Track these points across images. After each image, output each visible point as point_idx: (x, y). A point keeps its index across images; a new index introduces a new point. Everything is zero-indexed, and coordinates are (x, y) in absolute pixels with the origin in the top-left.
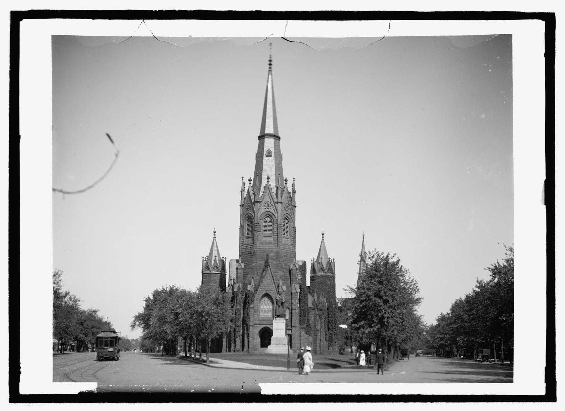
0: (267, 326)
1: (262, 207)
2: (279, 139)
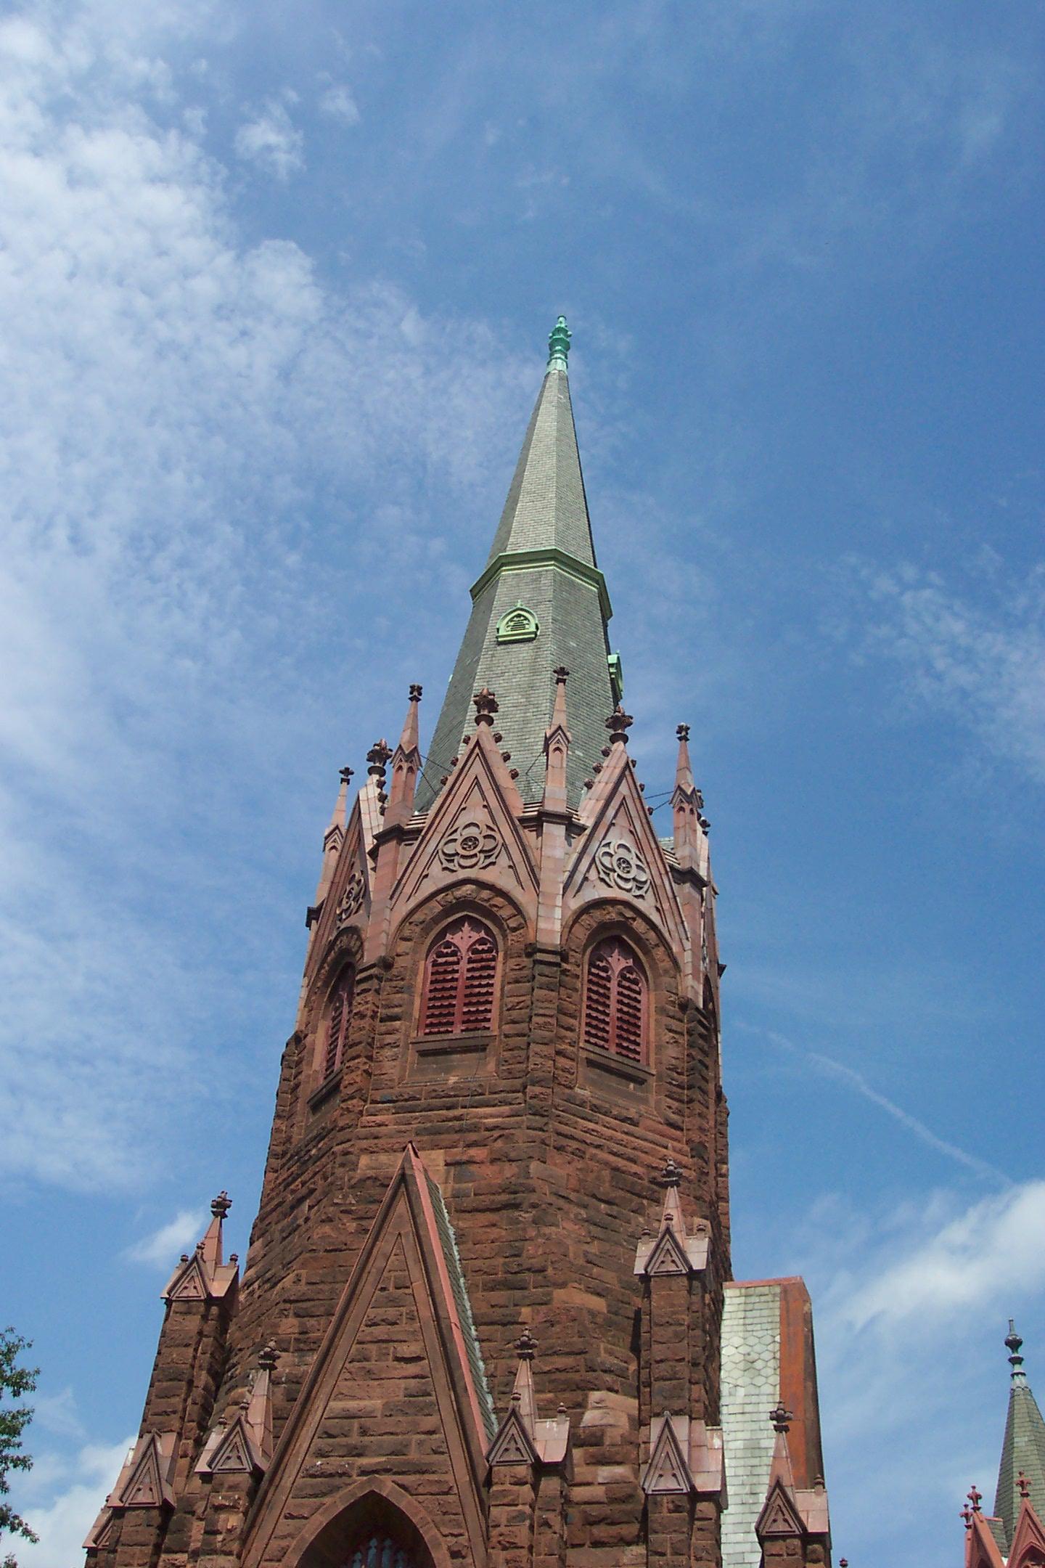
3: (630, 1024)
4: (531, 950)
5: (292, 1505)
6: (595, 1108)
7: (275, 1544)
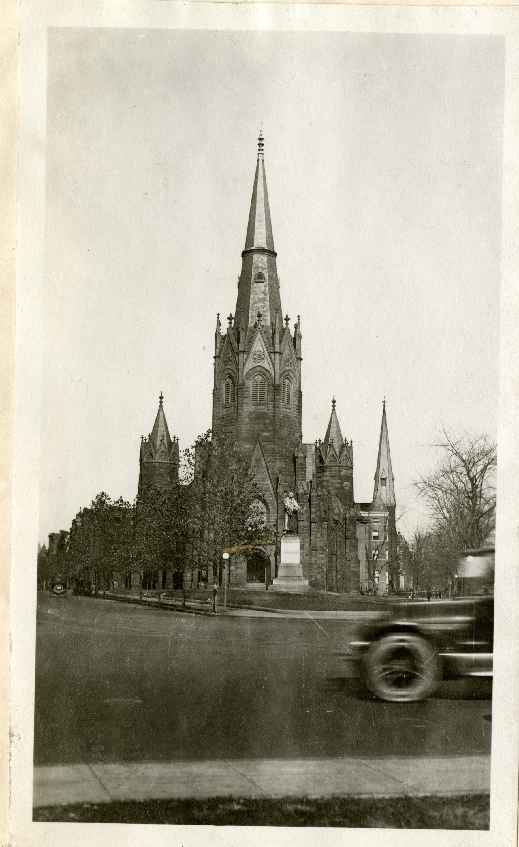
1: (251, 360)
2: (274, 256)
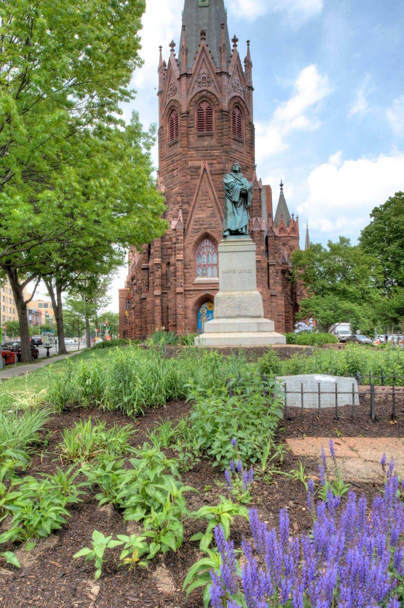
0: (207, 292)
3: (240, 129)
4: (222, 111)
5: (191, 234)
6: (235, 150)
7: (189, 241)
